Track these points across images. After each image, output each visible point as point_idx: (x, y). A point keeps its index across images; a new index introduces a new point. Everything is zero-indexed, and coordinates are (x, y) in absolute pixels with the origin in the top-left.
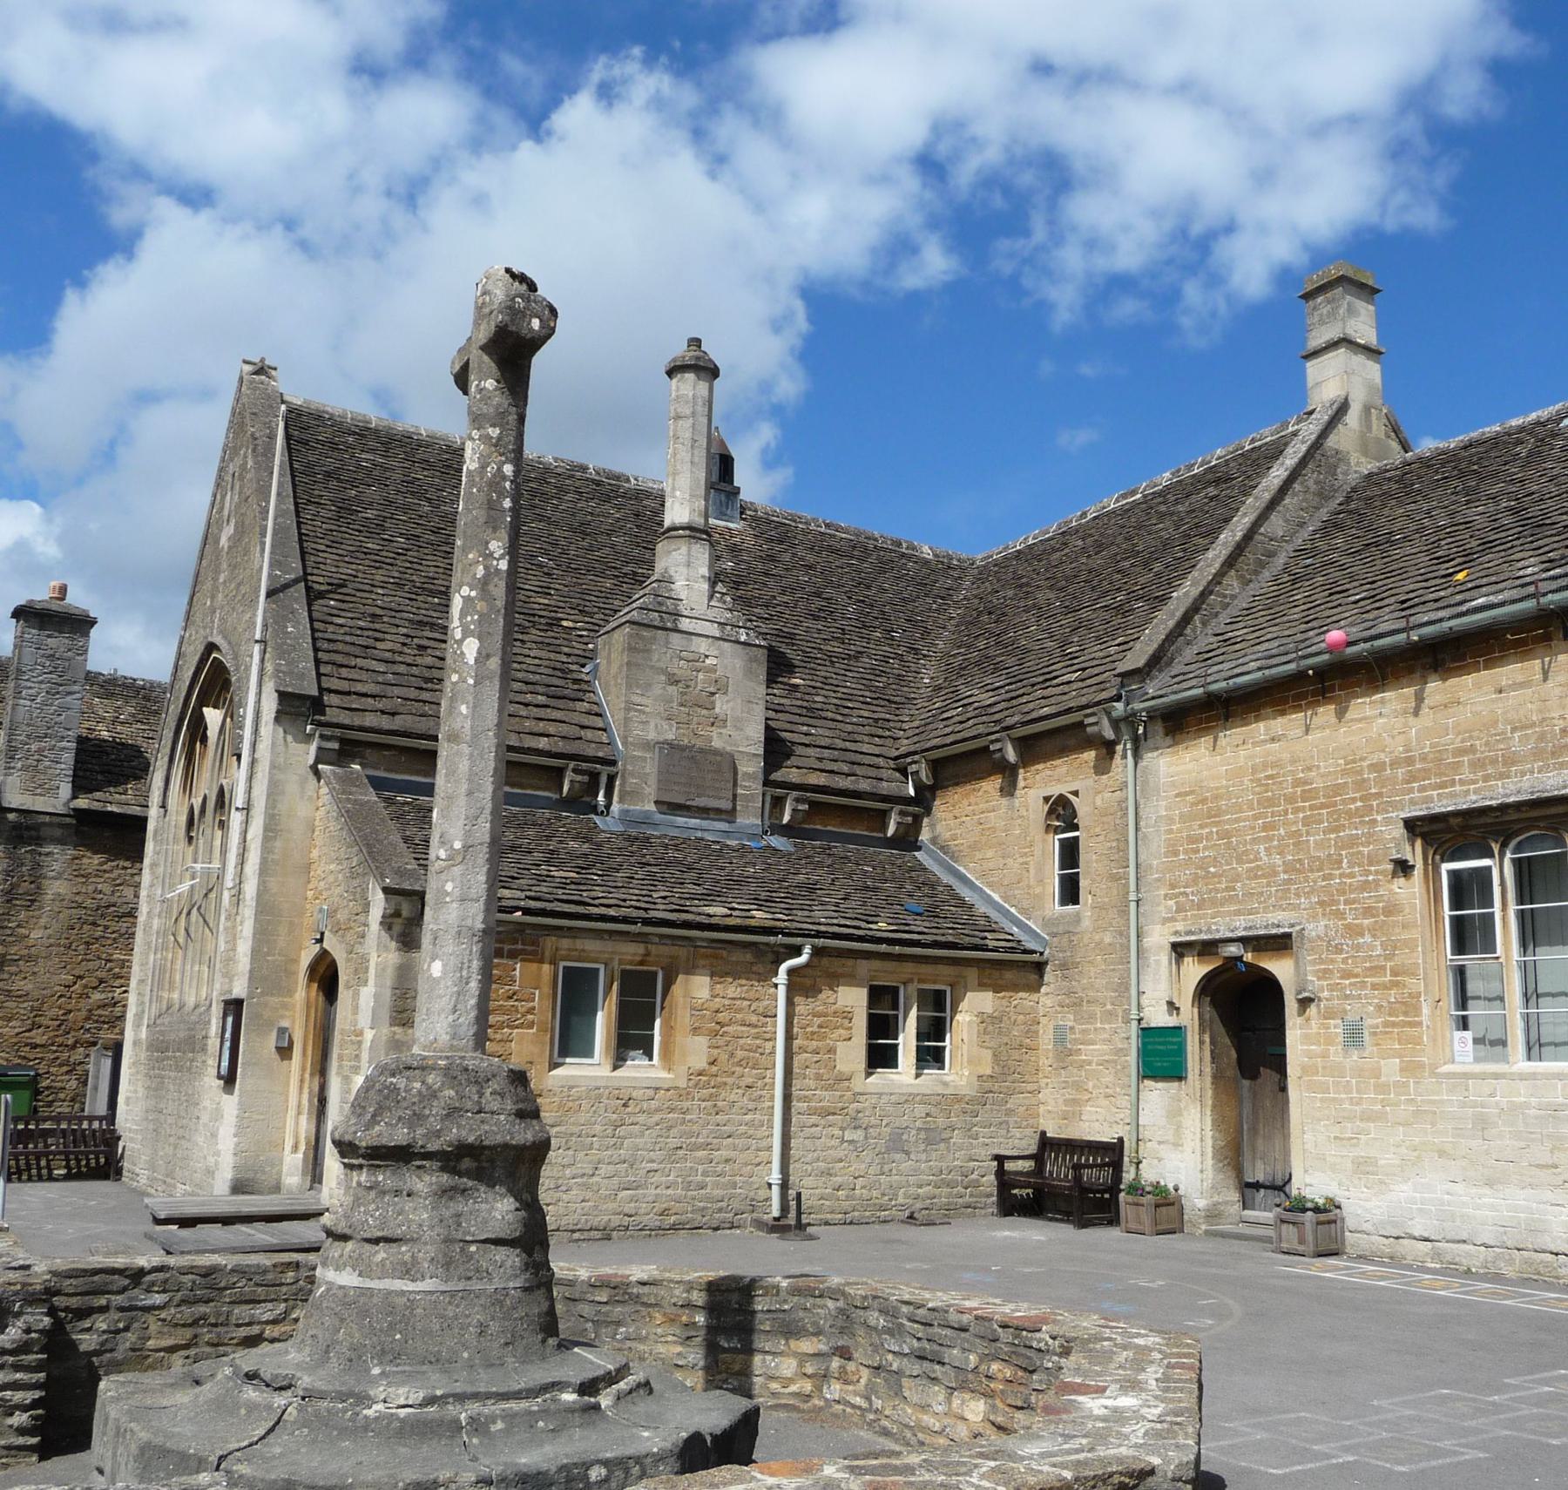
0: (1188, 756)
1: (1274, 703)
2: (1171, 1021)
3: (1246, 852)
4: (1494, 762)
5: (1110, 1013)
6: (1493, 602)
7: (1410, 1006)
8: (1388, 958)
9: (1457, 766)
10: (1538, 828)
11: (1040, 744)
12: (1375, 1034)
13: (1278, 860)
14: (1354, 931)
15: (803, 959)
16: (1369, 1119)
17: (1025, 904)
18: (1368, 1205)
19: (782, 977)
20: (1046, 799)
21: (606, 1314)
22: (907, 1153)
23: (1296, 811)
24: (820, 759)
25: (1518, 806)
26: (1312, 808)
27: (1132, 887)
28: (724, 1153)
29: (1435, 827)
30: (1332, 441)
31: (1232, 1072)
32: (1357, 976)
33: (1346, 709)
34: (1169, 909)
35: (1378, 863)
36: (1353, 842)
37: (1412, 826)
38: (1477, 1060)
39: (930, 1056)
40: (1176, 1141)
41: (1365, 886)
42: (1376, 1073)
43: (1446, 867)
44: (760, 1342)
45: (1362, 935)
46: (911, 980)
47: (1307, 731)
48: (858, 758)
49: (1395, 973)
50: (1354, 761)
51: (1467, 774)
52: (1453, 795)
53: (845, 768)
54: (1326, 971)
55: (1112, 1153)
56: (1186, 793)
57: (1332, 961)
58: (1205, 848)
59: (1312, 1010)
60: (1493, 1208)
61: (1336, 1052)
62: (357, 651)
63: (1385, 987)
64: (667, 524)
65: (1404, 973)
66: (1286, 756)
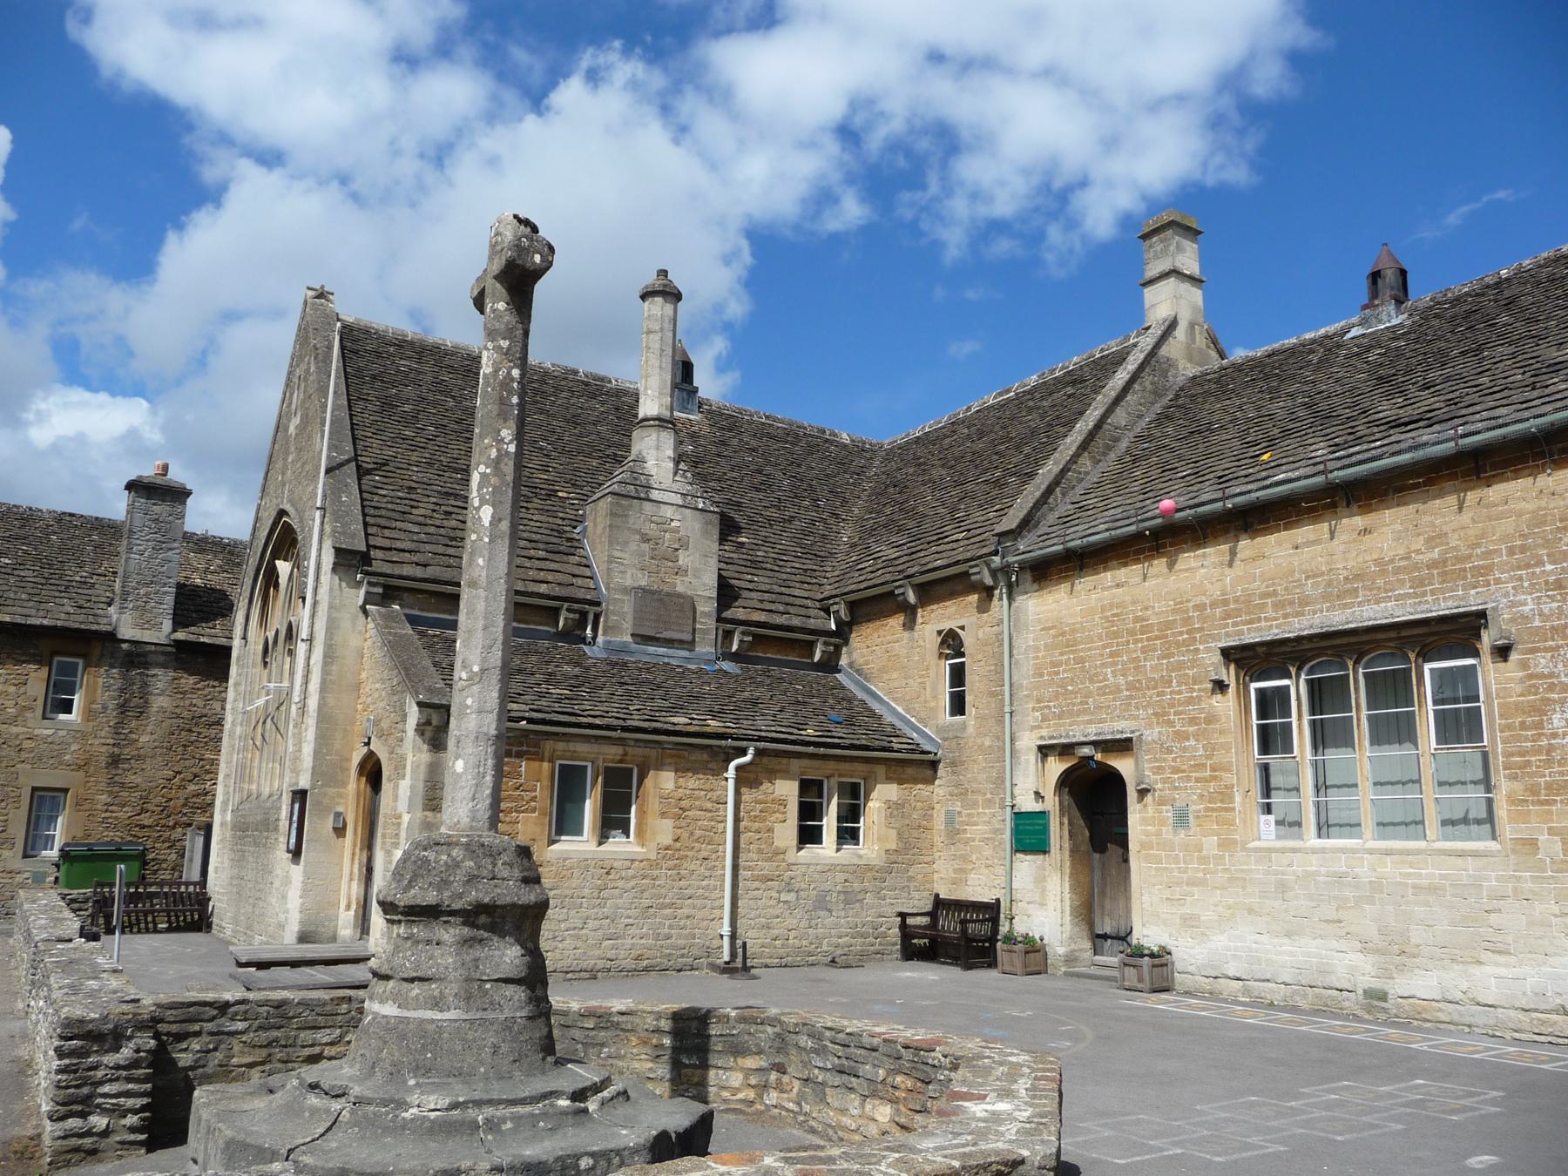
1: (1118, 557)
2: (1038, 807)
3: (1097, 674)
4: (1291, 603)
5: (989, 801)
6: (1291, 477)
7: (1225, 795)
8: (1208, 757)
9: (1262, 607)
11: (934, 589)
14: (1181, 736)
15: (748, 758)
16: (1193, 884)
17: (923, 715)
18: (1192, 952)
19: (731, 772)
20: (939, 632)
21: (593, 1038)
22: (830, 911)
23: (1136, 641)
24: (761, 601)
25: (1311, 638)
26: (1148, 639)
27: (1007, 701)
28: (685, 911)
30: (1164, 351)
31: (1086, 847)
34: (1036, 719)
35: (1201, 682)
36: (1180, 666)
37: (1230, 655)
38: (1278, 837)
39: (848, 835)
40: (1041, 902)
41: (1190, 701)
43: (1254, 686)
44: (714, 1060)
47: (1145, 578)
48: (791, 600)
49: (1213, 769)
51: (1270, 613)
52: (1259, 629)
53: (781, 608)
54: (1159, 768)
55: (991, 911)
57: (1165, 760)
59: (1149, 798)
60: (1291, 954)
62: (397, 516)
63: (1206, 780)
64: (641, 416)
65: (1221, 769)
66: (1128, 598)
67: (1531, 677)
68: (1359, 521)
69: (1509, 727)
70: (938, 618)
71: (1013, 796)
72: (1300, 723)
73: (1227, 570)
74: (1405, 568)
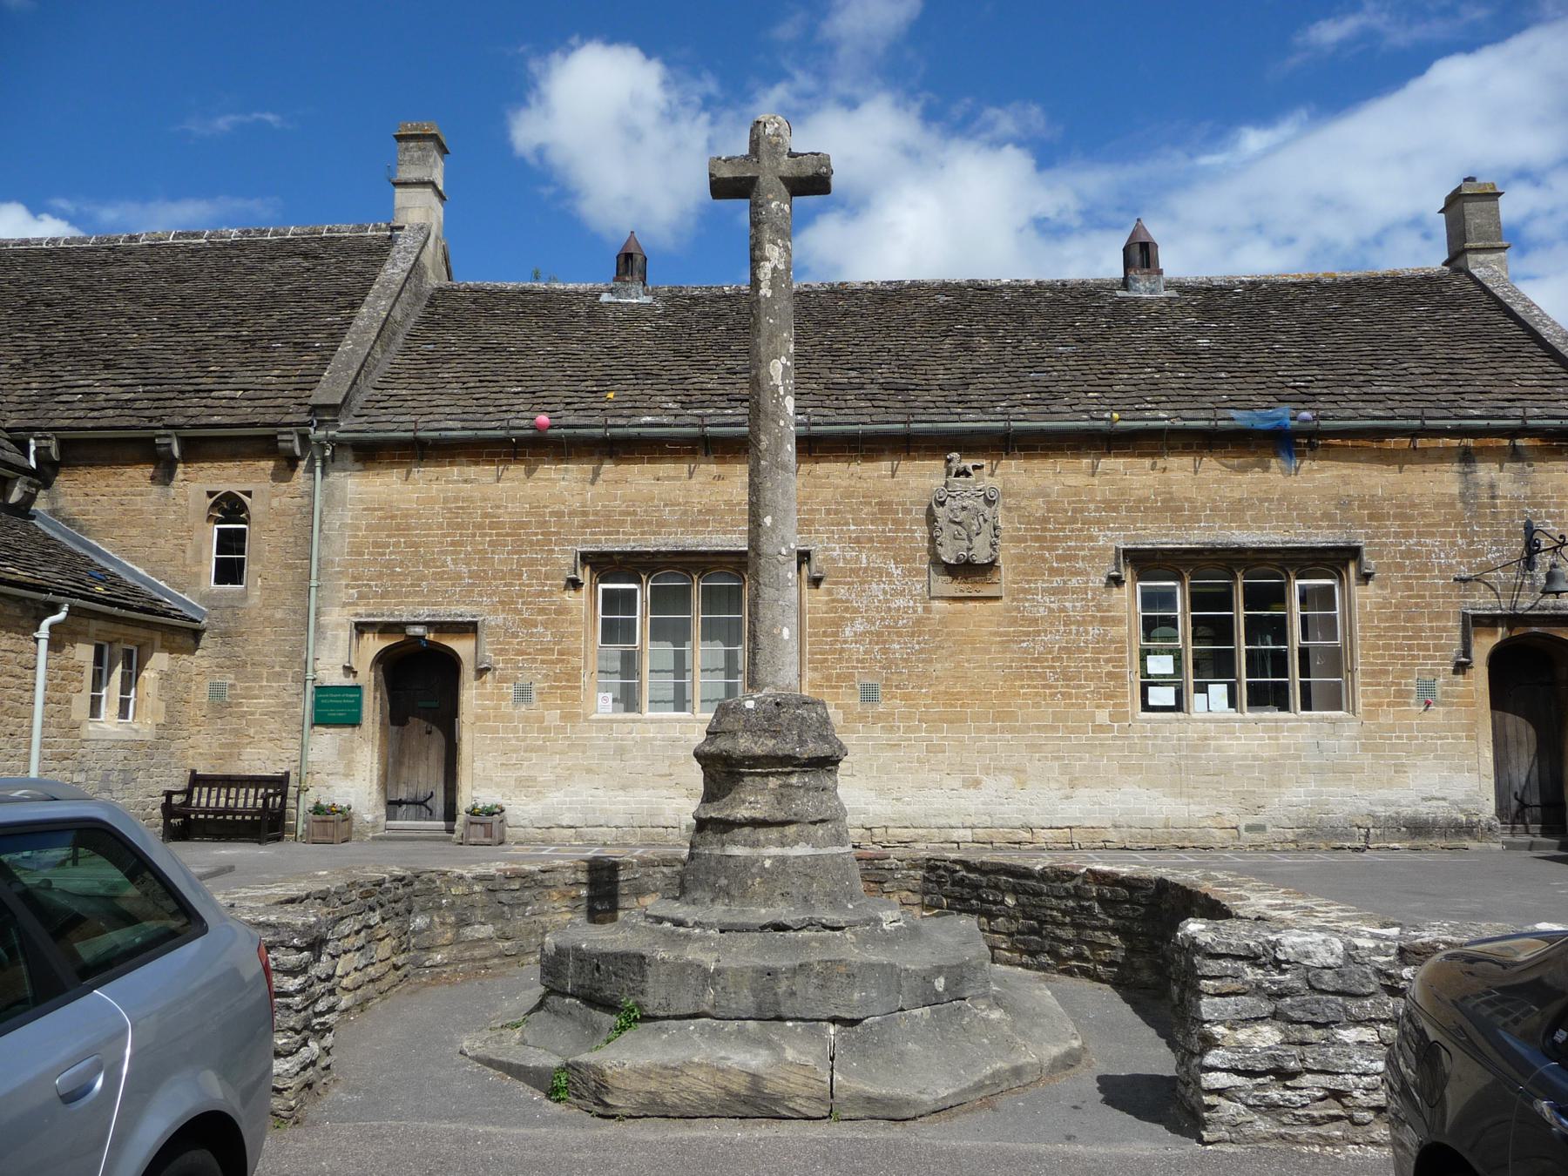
0: (378, 481)
1: (468, 455)
2: (349, 681)
5: (279, 674)
7: (573, 676)
11: (204, 446)
13: (464, 569)
20: (211, 494)
23: (483, 535)
26: (498, 535)
31: (388, 720)
36: (533, 562)
37: (586, 558)
40: (347, 772)
41: (540, 594)
42: (541, 720)
43: (601, 586)
44: (623, 903)
46: (118, 641)
49: (561, 653)
51: (628, 529)
55: (279, 783)
56: (375, 510)
59: (489, 676)
60: (626, 803)
63: (552, 662)
66: (477, 494)
67: (833, 601)
68: (714, 469)
69: (815, 634)
71: (315, 671)
72: (642, 617)
73: (588, 486)
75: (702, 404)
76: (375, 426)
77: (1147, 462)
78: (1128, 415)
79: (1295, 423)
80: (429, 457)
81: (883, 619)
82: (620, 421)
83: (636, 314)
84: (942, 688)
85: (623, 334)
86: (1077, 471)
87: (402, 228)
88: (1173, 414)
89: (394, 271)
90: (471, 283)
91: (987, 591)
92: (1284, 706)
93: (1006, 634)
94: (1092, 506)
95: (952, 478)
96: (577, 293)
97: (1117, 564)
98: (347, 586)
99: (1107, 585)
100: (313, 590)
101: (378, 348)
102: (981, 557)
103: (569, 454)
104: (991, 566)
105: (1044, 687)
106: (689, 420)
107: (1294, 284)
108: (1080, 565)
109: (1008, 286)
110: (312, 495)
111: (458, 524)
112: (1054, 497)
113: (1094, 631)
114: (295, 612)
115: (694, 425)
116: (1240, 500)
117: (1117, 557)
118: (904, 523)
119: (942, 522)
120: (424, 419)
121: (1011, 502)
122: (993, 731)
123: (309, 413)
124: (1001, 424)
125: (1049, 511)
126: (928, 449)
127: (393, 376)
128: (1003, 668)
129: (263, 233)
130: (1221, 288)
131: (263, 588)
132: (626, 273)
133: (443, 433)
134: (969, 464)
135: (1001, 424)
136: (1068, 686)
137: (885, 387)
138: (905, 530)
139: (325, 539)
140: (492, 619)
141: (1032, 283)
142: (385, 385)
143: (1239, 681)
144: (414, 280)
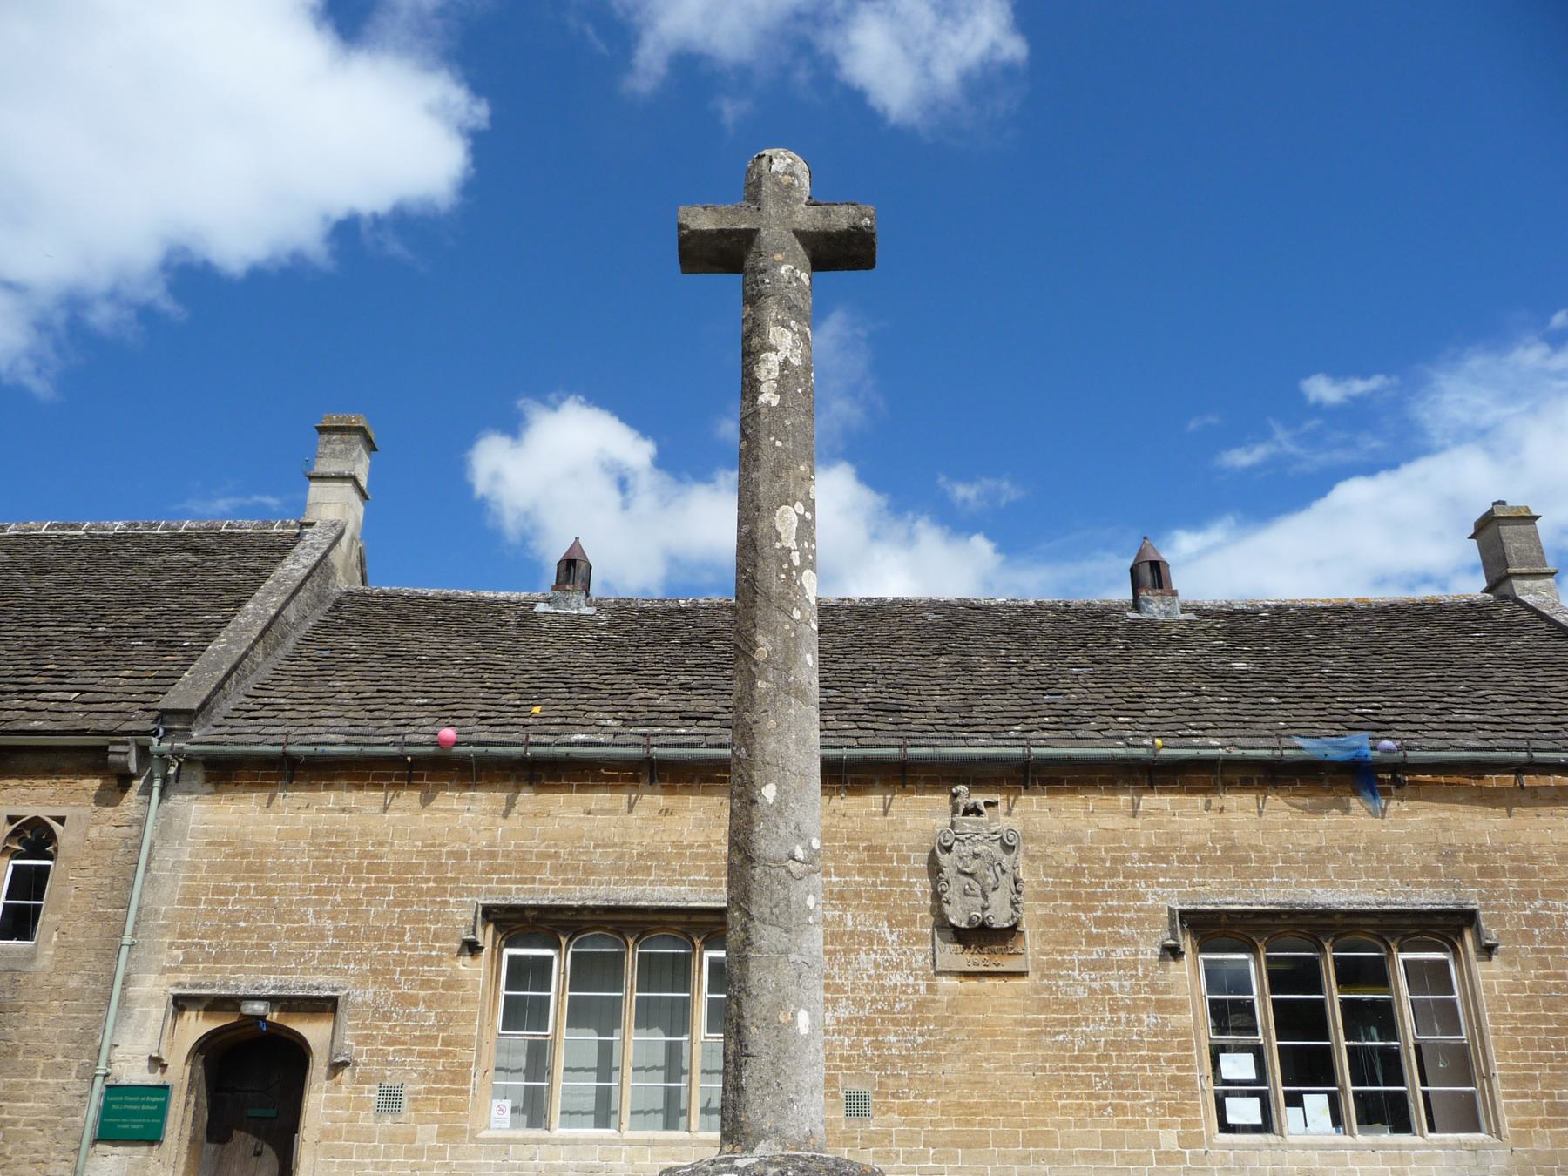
1: (349, 777)
2: (154, 1079)
3: (290, 912)
5: (60, 1067)
7: (459, 1075)
8: (440, 1029)
9: (539, 868)
10: (605, 929)
12: (415, 1100)
13: (328, 924)
14: (407, 1001)
20: (12, 820)
25: (594, 910)
26: (377, 880)
29: (510, 916)
30: (331, 556)
31: (202, 1136)
32: (404, 1043)
33: (432, 798)
34: (175, 959)
35: (446, 940)
36: (419, 918)
38: (513, 1126)
41: (426, 960)
42: (411, 1138)
43: (507, 952)
45: (416, 1005)
47: (385, 809)
49: (446, 1043)
50: (433, 845)
51: (547, 876)
52: (530, 891)
56: (222, 844)
57: (378, 1028)
58: (235, 902)
59: (346, 1074)
61: (366, 1117)
63: (434, 1056)
65: (456, 1044)
66: (356, 828)
68: (660, 800)
70: (33, 798)
72: (558, 994)
73: (499, 820)
74: (703, 855)
75: (649, 722)
76: (237, 738)
77: (1200, 800)
78: (1171, 742)
79: (1376, 754)
80: (301, 779)
81: (874, 1001)
82: (545, 739)
83: (574, 626)
84: (954, 1098)
85: (559, 645)
86: (1114, 811)
87: (311, 525)
88: (1225, 741)
89: (294, 567)
90: (387, 589)
91: (1009, 965)
92: (1402, 1124)
93: (1036, 1023)
94: (1135, 855)
95: (959, 817)
96: (509, 602)
97: (1173, 931)
98: (171, 945)
99: (1162, 958)
100: (125, 950)
101: (259, 649)
102: (1000, 919)
103: (479, 779)
104: (1012, 932)
105: (1090, 1096)
106: (631, 739)
107: (1325, 609)
108: (1125, 930)
109: (1004, 605)
110: (142, 823)
111: (327, 865)
112: (1087, 843)
113: (1149, 1019)
114: (96, 979)
115: (637, 745)
116: (1319, 849)
117: (1172, 921)
118: (899, 874)
119: (949, 872)
120: (300, 731)
121: (1034, 848)
122: (1024, 1159)
123: (156, 720)
124: (1019, 750)
125: (1082, 860)
126: (927, 780)
127: (275, 682)
128: (1033, 1070)
129: (151, 526)
130: (1244, 612)
131: (59, 946)
132: (567, 581)
133: (320, 748)
134: (979, 799)
135: (1019, 750)
136: (1120, 1096)
137: (872, 707)
138: (901, 884)
139: (152, 881)
140: (358, 993)
141: (1031, 602)
142: (261, 693)
143: (1343, 1089)
144: (317, 579)
